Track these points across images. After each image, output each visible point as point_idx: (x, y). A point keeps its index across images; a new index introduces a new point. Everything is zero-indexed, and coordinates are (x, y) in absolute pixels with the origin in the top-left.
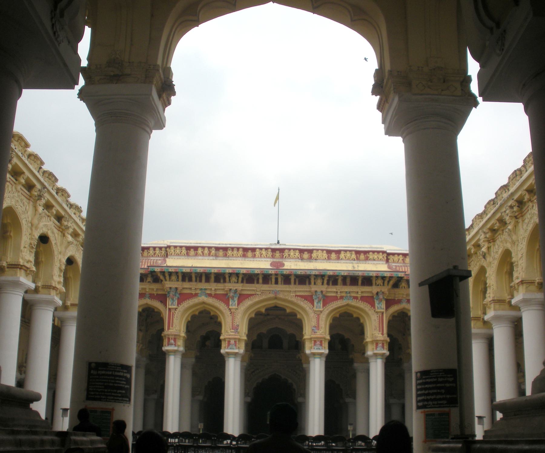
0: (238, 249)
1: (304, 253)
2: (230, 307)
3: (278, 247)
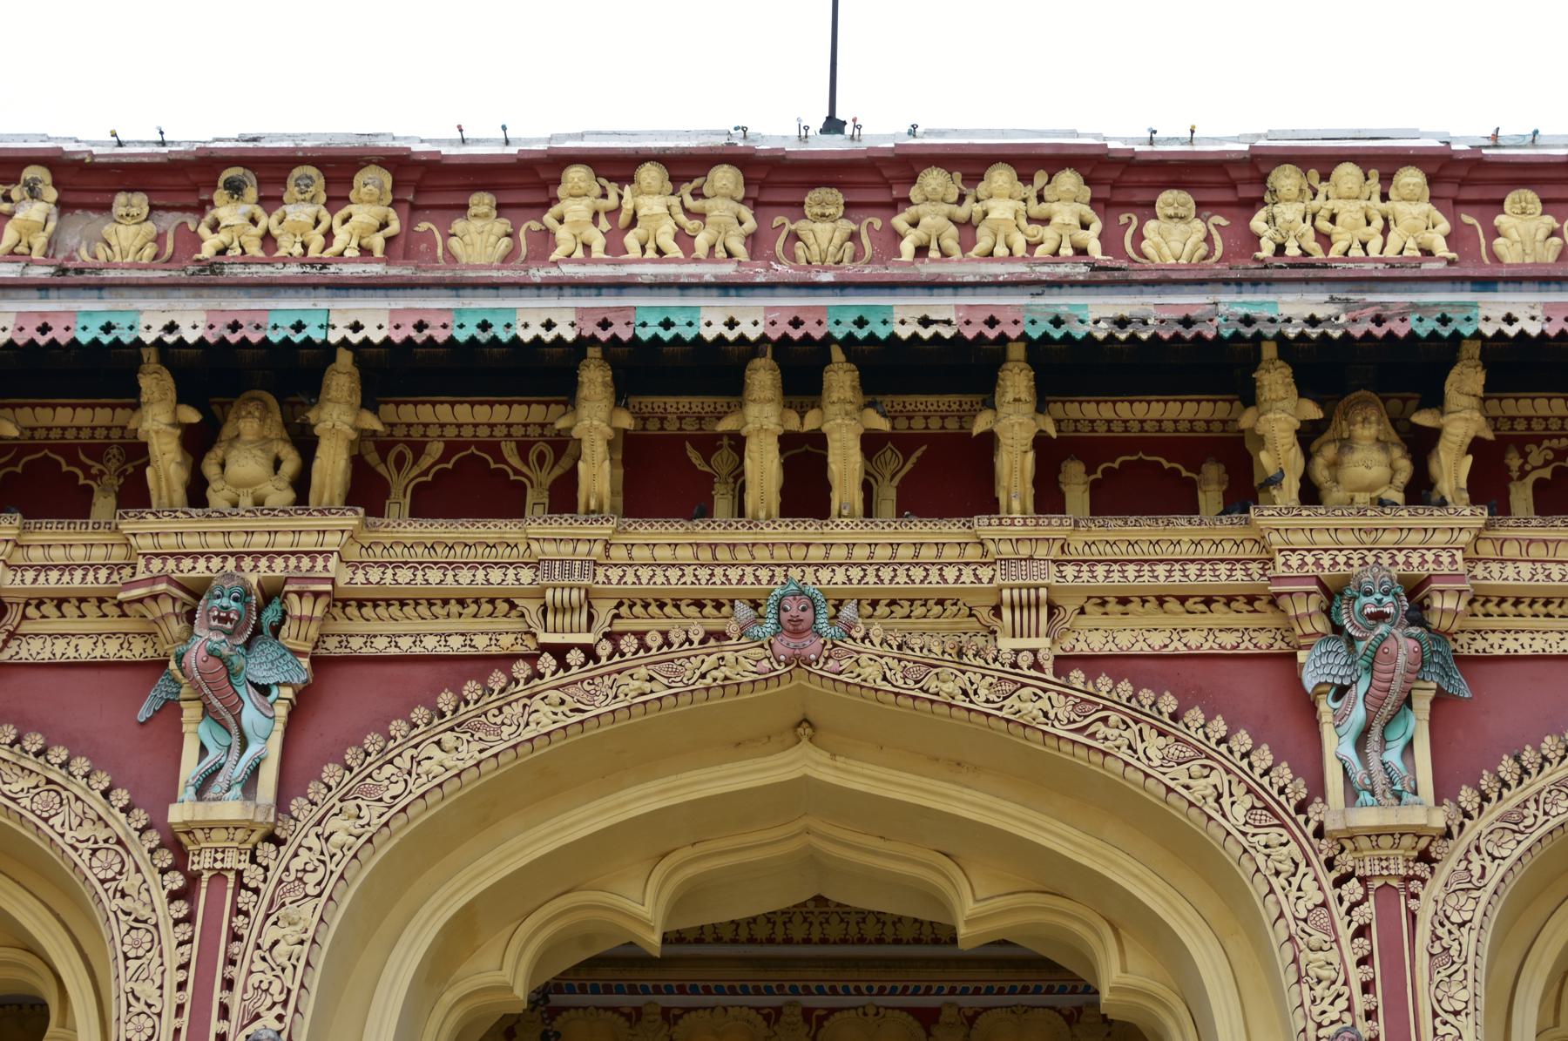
0: (338, 169)
1: (1147, 209)
2: (177, 814)
3: (834, 144)
